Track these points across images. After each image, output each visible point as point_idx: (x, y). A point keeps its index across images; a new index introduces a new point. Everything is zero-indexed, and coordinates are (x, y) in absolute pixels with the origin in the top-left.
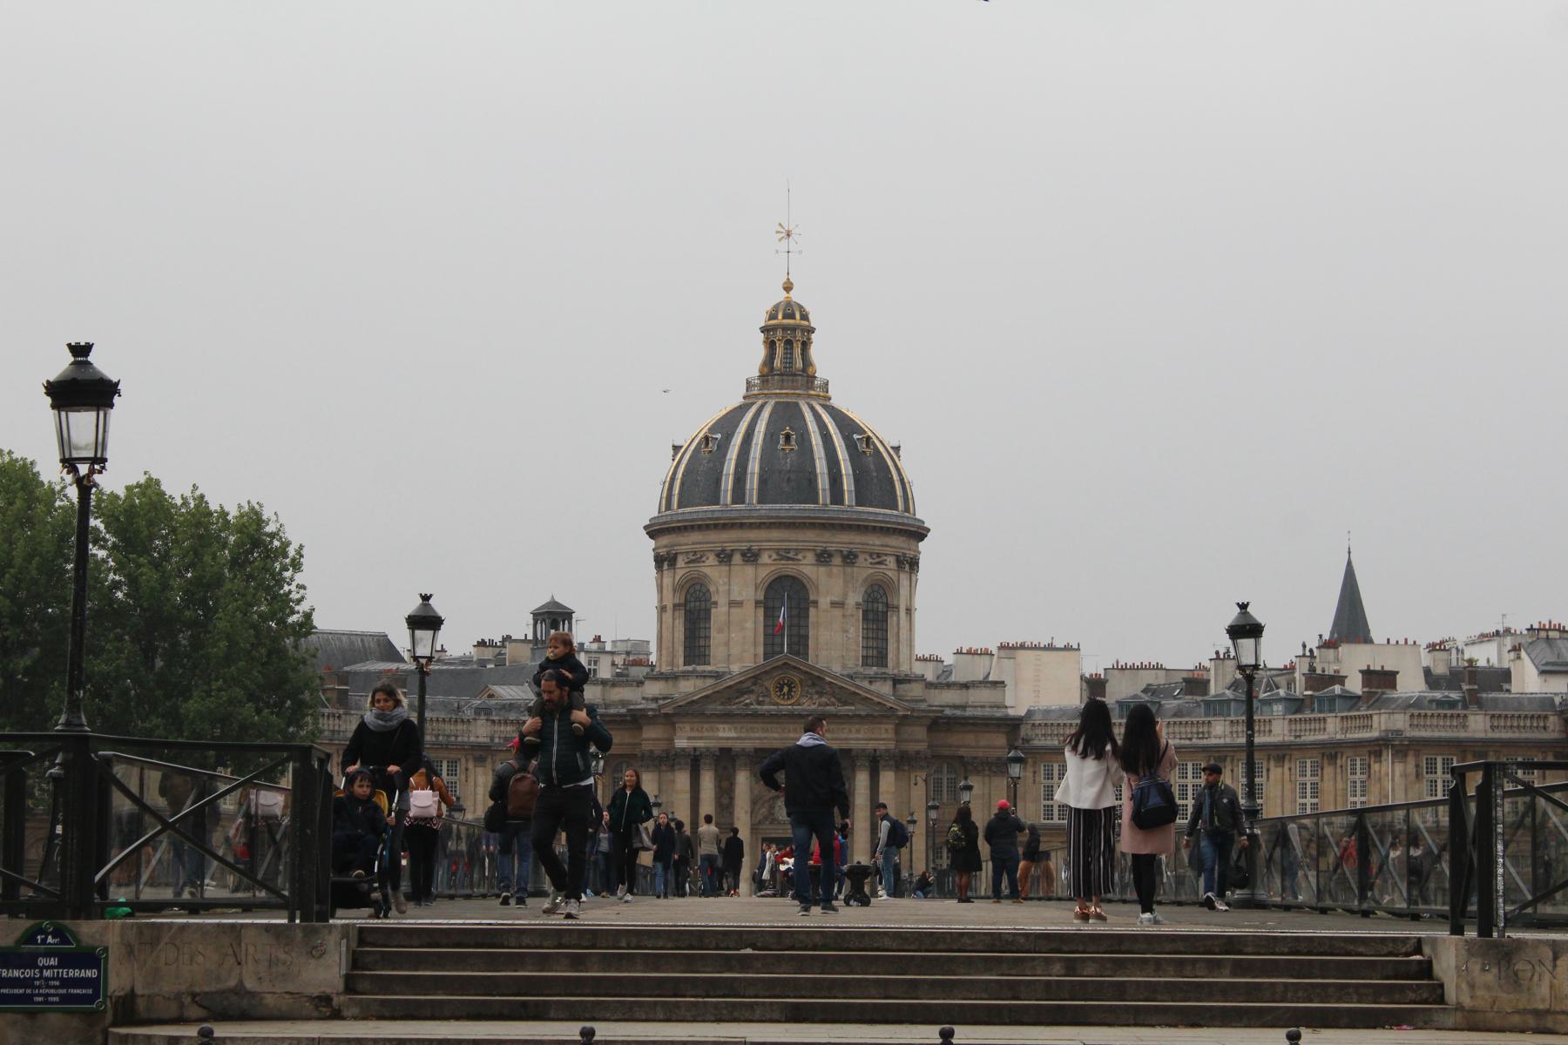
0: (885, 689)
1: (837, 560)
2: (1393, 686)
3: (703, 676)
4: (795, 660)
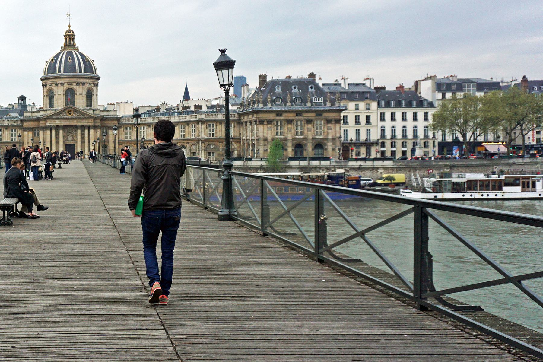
0: (91, 112)
1: (81, 85)
2: (201, 109)
3: (52, 110)
4: (72, 106)
